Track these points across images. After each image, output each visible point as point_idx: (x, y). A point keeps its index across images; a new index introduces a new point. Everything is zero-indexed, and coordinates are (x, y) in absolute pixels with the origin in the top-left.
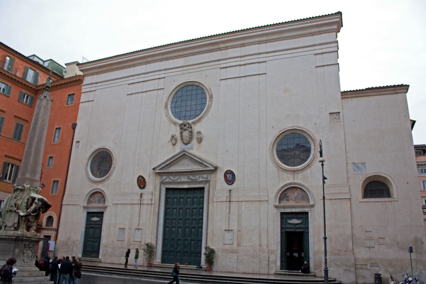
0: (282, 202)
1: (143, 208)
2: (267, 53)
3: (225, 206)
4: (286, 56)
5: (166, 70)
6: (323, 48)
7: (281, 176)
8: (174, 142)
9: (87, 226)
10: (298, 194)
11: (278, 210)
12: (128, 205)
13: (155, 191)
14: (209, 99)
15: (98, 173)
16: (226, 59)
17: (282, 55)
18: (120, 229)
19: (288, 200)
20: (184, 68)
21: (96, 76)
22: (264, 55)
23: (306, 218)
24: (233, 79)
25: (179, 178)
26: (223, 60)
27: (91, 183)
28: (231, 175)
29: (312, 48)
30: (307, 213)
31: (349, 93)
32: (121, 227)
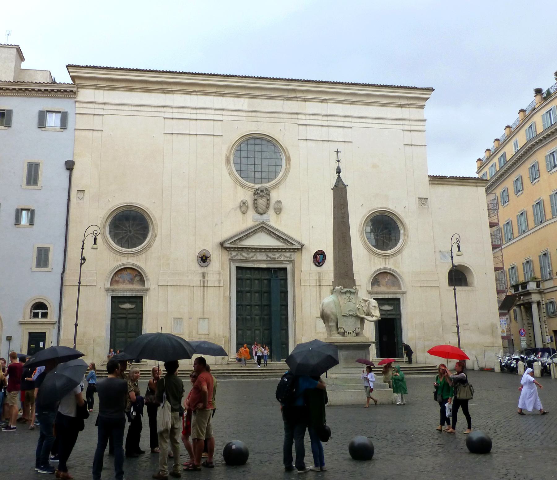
1: (207, 291)
2: (353, 117)
3: (314, 290)
4: (373, 126)
5: (224, 110)
6: (412, 125)
7: (373, 261)
8: (244, 209)
9: (114, 316)
10: (389, 279)
12: (184, 287)
14: (286, 160)
16: (305, 114)
17: (369, 123)
18: (174, 318)
19: (379, 286)
20: (250, 114)
21: (102, 92)
22: (350, 119)
23: (397, 304)
24: (314, 141)
27: (115, 255)
28: (322, 255)
29: (401, 122)
30: (398, 300)
32: (176, 317)
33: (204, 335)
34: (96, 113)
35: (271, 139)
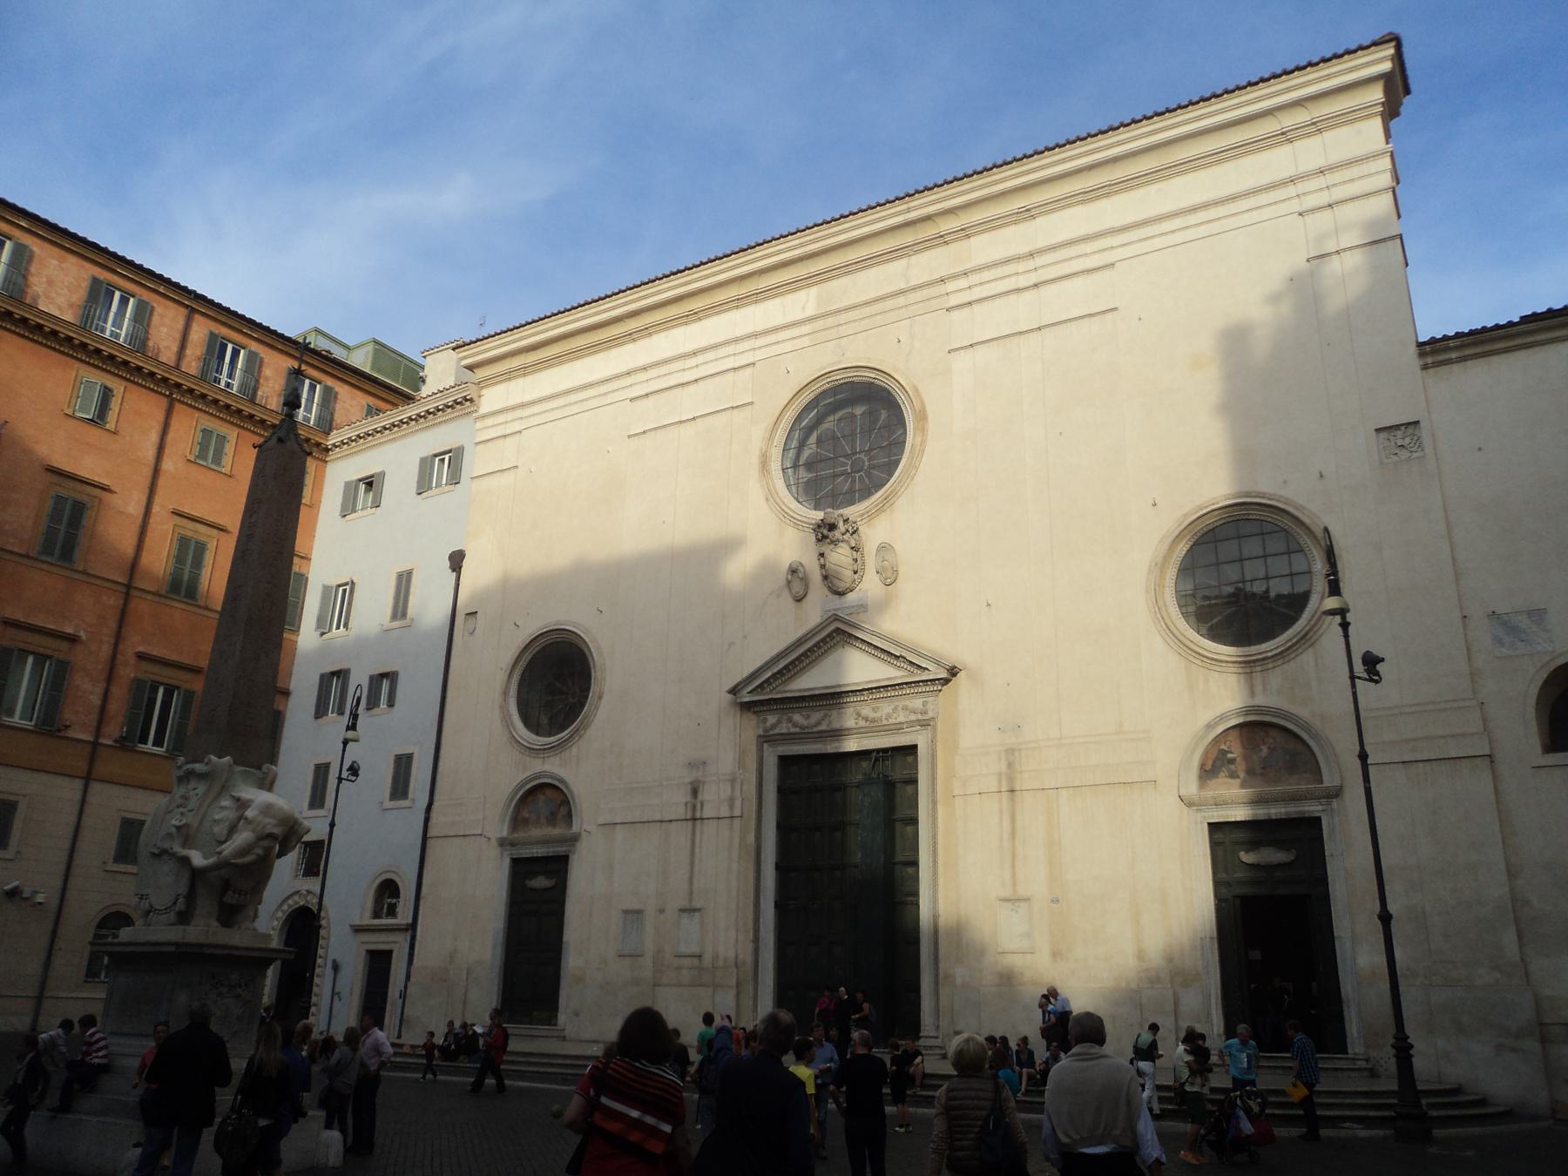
0: (1213, 783)
6: (1334, 185)
8: (797, 587)
11: (1199, 815)
12: (651, 824)
13: (741, 771)
15: (544, 720)
18: (626, 912)
20: (820, 324)
21: (521, 381)
25: (825, 716)
26: (955, 277)
29: (1291, 190)
30: (1317, 821)
31: (1451, 342)
33: (689, 959)
34: (508, 432)
35: (873, 376)
